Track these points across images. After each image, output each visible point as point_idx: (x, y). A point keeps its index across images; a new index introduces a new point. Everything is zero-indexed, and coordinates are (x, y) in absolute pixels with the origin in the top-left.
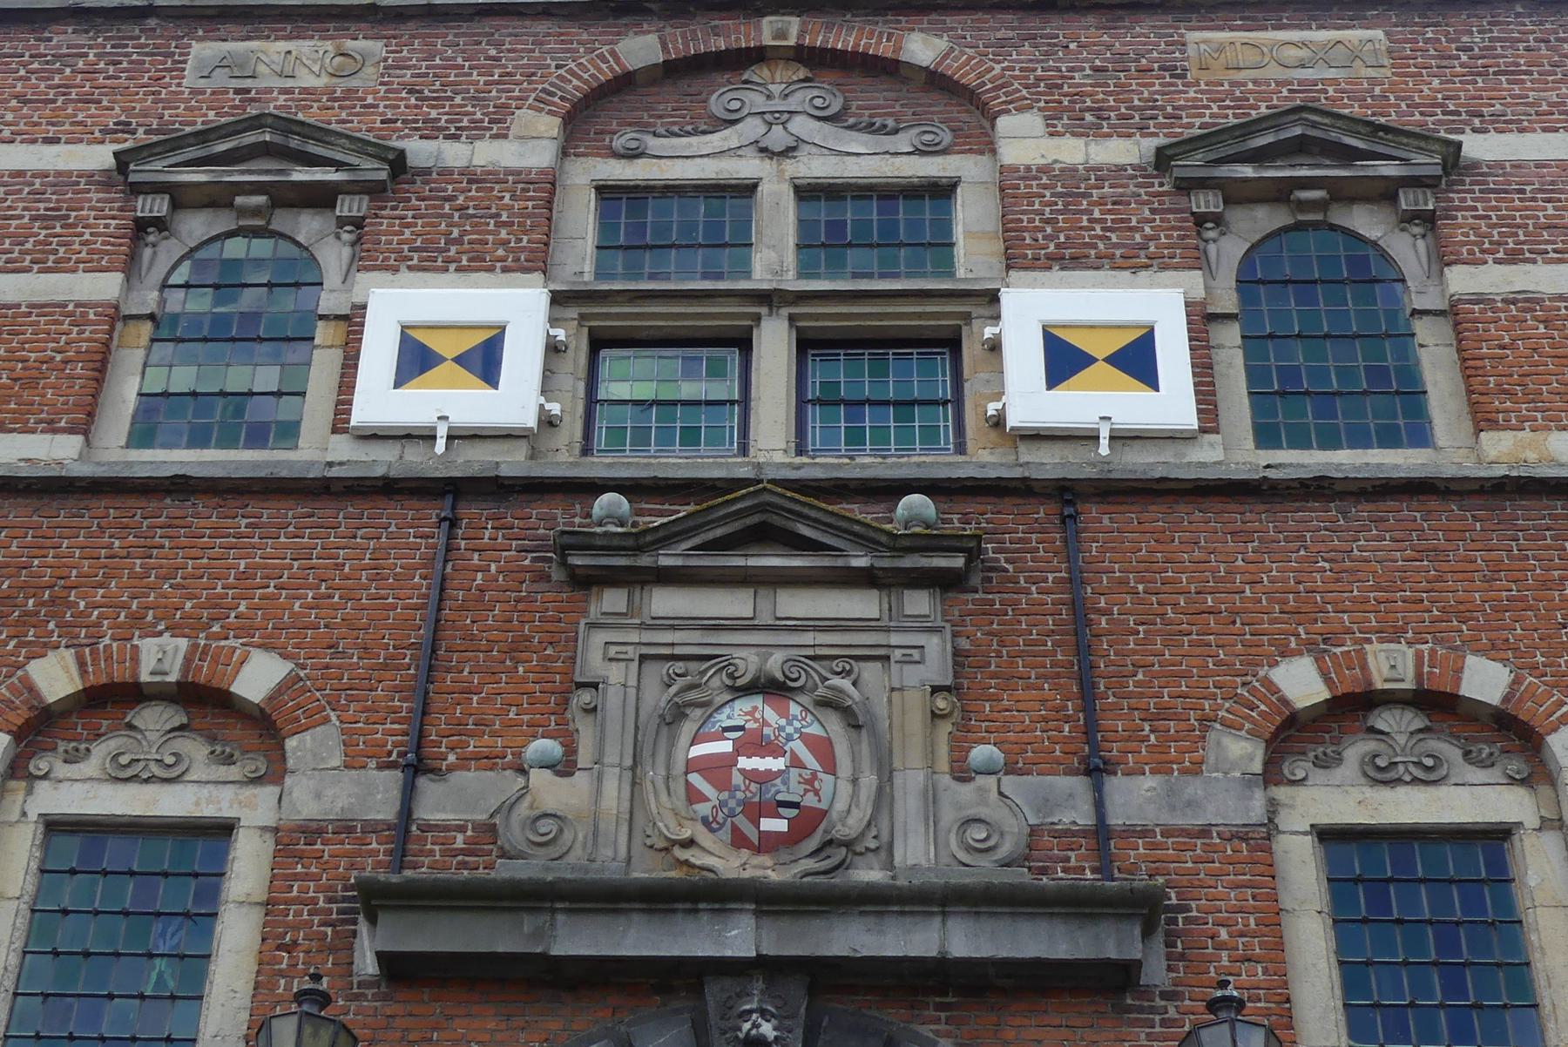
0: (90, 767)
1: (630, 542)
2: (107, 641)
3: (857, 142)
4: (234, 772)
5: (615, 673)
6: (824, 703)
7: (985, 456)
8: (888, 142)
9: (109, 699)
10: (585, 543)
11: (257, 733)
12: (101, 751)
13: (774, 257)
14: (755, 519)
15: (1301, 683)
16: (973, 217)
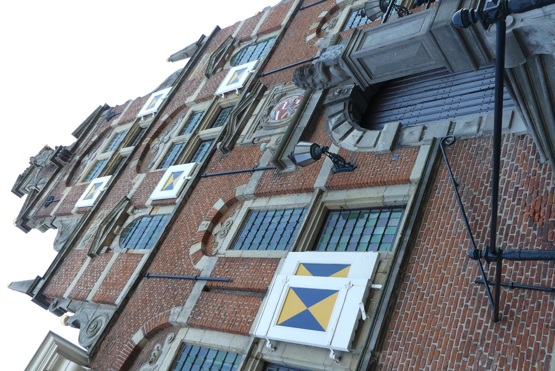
1: (229, 136)
2: (193, 239)
3: (176, 127)
4: (237, 211)
5: (254, 136)
6: (279, 100)
8: (178, 123)
9: (207, 238)
12: (218, 239)
14: (236, 117)
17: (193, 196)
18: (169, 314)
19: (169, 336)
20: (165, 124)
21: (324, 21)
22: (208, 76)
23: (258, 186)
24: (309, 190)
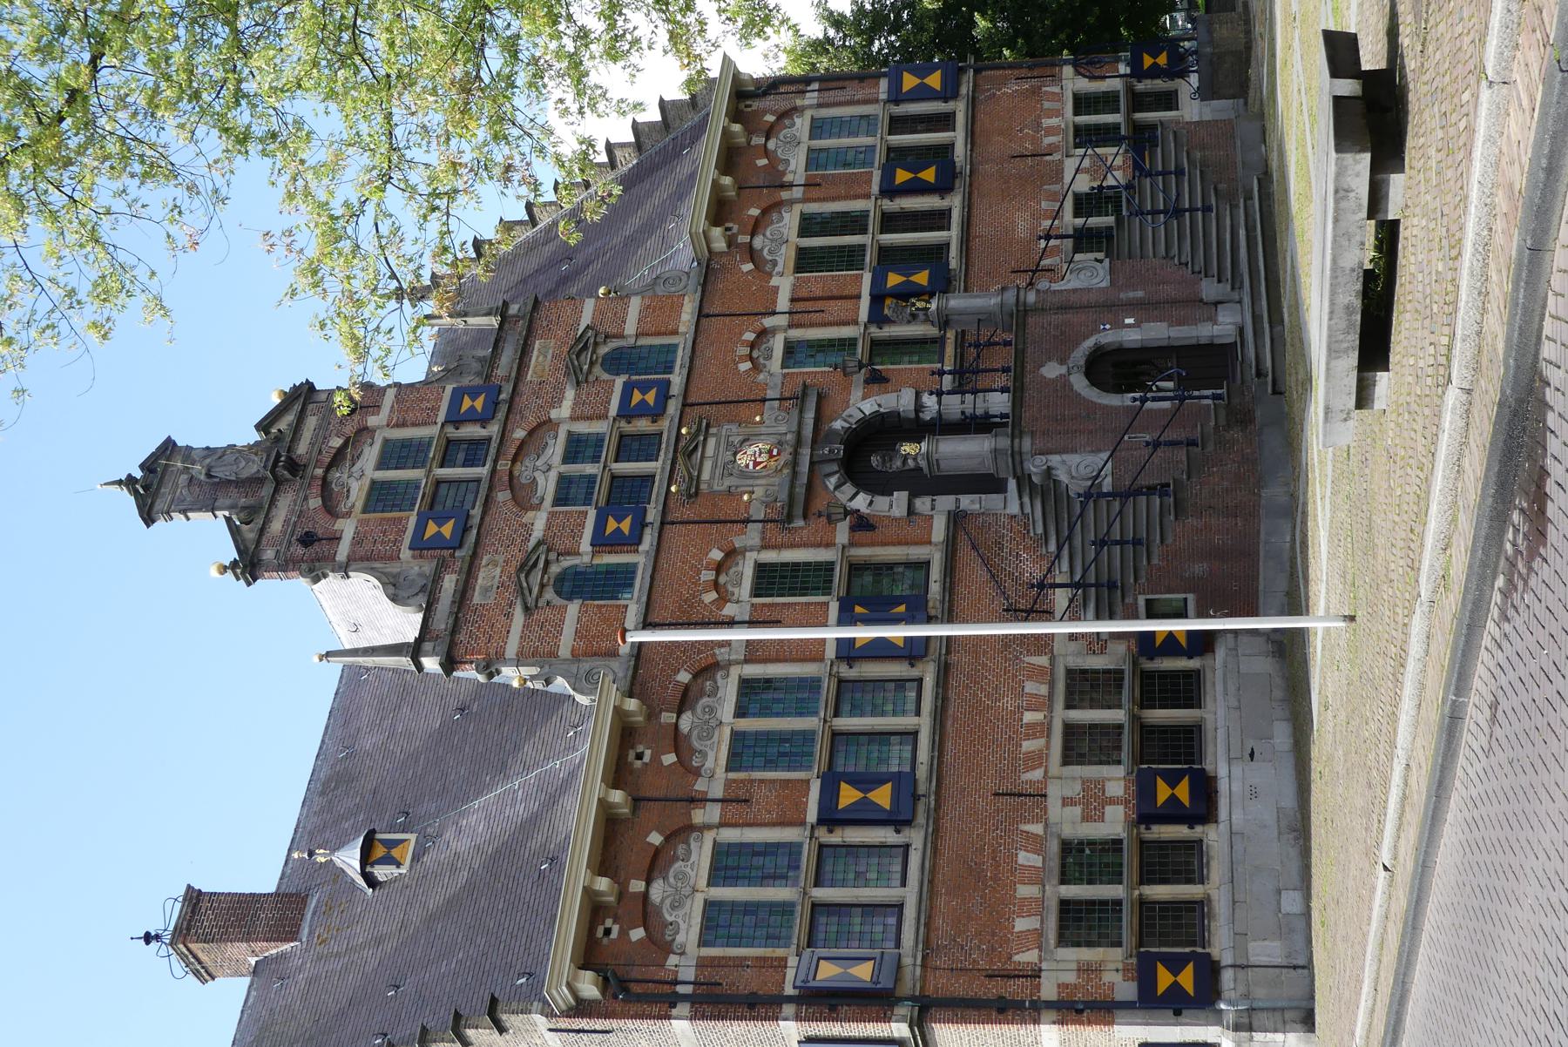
0: (736, 591)
3: (549, 451)
7: (666, 423)
9: (716, 585)
10: (689, 488)
11: (731, 554)
12: (730, 589)
13: (590, 469)
15: (745, 366)
16: (583, 428)
17: (665, 545)
18: (714, 655)
19: (719, 675)
20: (523, 443)
21: (752, 345)
22: (578, 383)
23: (763, 539)
24: (829, 545)
